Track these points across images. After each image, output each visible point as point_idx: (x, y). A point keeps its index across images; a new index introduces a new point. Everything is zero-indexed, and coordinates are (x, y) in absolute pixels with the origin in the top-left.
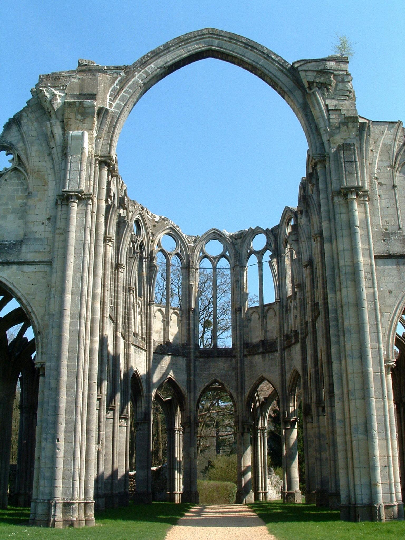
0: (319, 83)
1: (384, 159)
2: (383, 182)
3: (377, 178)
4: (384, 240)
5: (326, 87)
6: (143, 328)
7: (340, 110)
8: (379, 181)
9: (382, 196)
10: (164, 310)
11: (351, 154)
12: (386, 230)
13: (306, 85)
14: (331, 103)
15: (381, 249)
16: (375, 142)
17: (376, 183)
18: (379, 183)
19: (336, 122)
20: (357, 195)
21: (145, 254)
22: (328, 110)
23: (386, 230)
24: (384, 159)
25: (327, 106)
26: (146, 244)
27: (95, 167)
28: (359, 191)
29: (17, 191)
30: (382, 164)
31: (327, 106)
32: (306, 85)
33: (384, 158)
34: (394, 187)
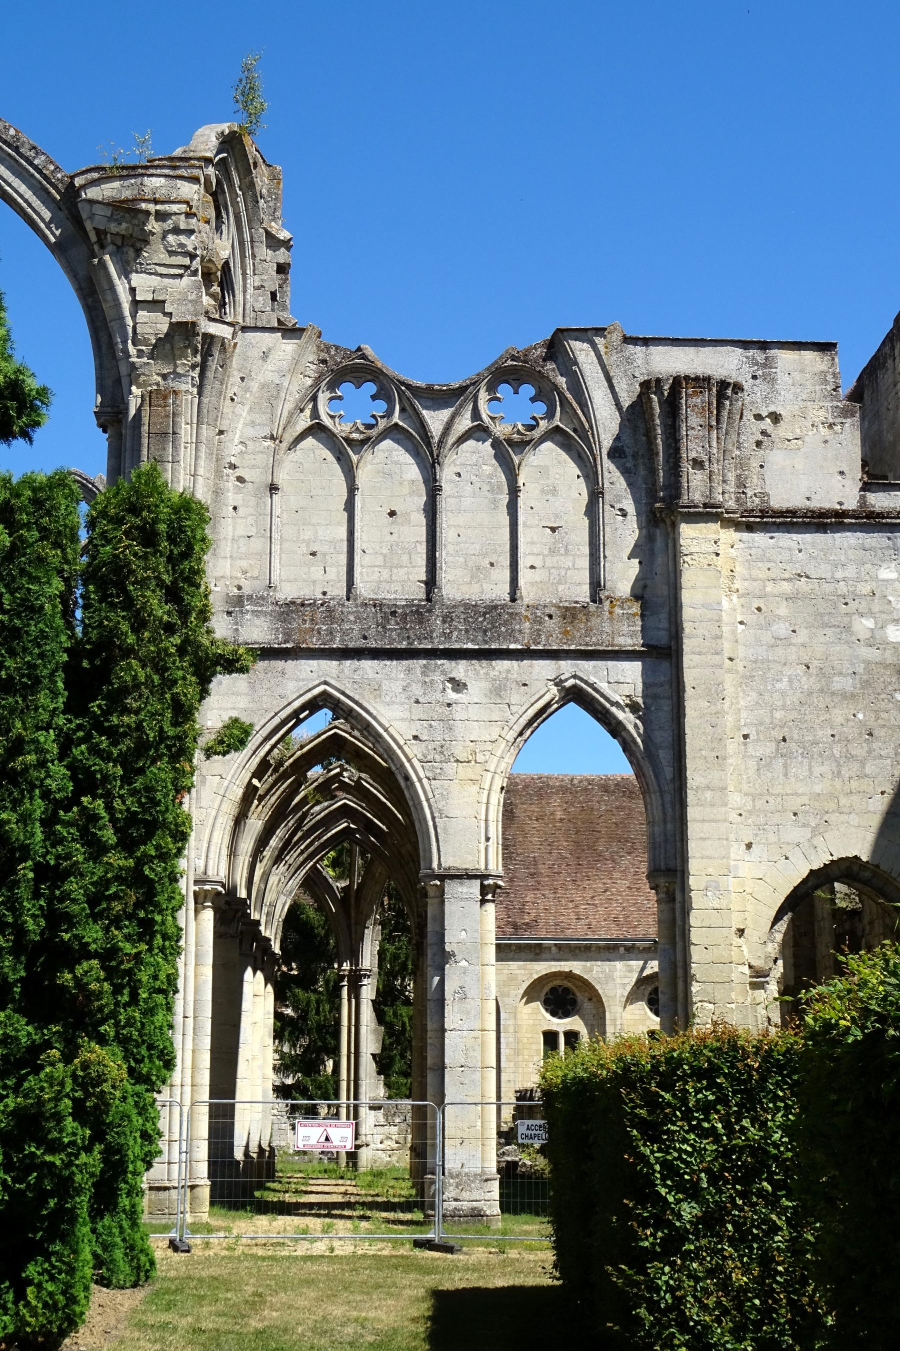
0: (117, 234)
1: (257, 421)
2: (246, 478)
3: (233, 467)
4: (229, 613)
5: (133, 246)
7: (164, 302)
8: (238, 472)
9: (241, 510)
11: (167, 416)
12: (239, 588)
13: (93, 238)
14: (145, 284)
16: (242, 379)
17: (233, 478)
18: (240, 479)
19: (151, 331)
22: (136, 305)
23: (239, 588)
24: (257, 421)
25: (133, 290)
30: (251, 432)
31: (133, 290)
32: (93, 238)
33: (259, 418)
34: (273, 488)
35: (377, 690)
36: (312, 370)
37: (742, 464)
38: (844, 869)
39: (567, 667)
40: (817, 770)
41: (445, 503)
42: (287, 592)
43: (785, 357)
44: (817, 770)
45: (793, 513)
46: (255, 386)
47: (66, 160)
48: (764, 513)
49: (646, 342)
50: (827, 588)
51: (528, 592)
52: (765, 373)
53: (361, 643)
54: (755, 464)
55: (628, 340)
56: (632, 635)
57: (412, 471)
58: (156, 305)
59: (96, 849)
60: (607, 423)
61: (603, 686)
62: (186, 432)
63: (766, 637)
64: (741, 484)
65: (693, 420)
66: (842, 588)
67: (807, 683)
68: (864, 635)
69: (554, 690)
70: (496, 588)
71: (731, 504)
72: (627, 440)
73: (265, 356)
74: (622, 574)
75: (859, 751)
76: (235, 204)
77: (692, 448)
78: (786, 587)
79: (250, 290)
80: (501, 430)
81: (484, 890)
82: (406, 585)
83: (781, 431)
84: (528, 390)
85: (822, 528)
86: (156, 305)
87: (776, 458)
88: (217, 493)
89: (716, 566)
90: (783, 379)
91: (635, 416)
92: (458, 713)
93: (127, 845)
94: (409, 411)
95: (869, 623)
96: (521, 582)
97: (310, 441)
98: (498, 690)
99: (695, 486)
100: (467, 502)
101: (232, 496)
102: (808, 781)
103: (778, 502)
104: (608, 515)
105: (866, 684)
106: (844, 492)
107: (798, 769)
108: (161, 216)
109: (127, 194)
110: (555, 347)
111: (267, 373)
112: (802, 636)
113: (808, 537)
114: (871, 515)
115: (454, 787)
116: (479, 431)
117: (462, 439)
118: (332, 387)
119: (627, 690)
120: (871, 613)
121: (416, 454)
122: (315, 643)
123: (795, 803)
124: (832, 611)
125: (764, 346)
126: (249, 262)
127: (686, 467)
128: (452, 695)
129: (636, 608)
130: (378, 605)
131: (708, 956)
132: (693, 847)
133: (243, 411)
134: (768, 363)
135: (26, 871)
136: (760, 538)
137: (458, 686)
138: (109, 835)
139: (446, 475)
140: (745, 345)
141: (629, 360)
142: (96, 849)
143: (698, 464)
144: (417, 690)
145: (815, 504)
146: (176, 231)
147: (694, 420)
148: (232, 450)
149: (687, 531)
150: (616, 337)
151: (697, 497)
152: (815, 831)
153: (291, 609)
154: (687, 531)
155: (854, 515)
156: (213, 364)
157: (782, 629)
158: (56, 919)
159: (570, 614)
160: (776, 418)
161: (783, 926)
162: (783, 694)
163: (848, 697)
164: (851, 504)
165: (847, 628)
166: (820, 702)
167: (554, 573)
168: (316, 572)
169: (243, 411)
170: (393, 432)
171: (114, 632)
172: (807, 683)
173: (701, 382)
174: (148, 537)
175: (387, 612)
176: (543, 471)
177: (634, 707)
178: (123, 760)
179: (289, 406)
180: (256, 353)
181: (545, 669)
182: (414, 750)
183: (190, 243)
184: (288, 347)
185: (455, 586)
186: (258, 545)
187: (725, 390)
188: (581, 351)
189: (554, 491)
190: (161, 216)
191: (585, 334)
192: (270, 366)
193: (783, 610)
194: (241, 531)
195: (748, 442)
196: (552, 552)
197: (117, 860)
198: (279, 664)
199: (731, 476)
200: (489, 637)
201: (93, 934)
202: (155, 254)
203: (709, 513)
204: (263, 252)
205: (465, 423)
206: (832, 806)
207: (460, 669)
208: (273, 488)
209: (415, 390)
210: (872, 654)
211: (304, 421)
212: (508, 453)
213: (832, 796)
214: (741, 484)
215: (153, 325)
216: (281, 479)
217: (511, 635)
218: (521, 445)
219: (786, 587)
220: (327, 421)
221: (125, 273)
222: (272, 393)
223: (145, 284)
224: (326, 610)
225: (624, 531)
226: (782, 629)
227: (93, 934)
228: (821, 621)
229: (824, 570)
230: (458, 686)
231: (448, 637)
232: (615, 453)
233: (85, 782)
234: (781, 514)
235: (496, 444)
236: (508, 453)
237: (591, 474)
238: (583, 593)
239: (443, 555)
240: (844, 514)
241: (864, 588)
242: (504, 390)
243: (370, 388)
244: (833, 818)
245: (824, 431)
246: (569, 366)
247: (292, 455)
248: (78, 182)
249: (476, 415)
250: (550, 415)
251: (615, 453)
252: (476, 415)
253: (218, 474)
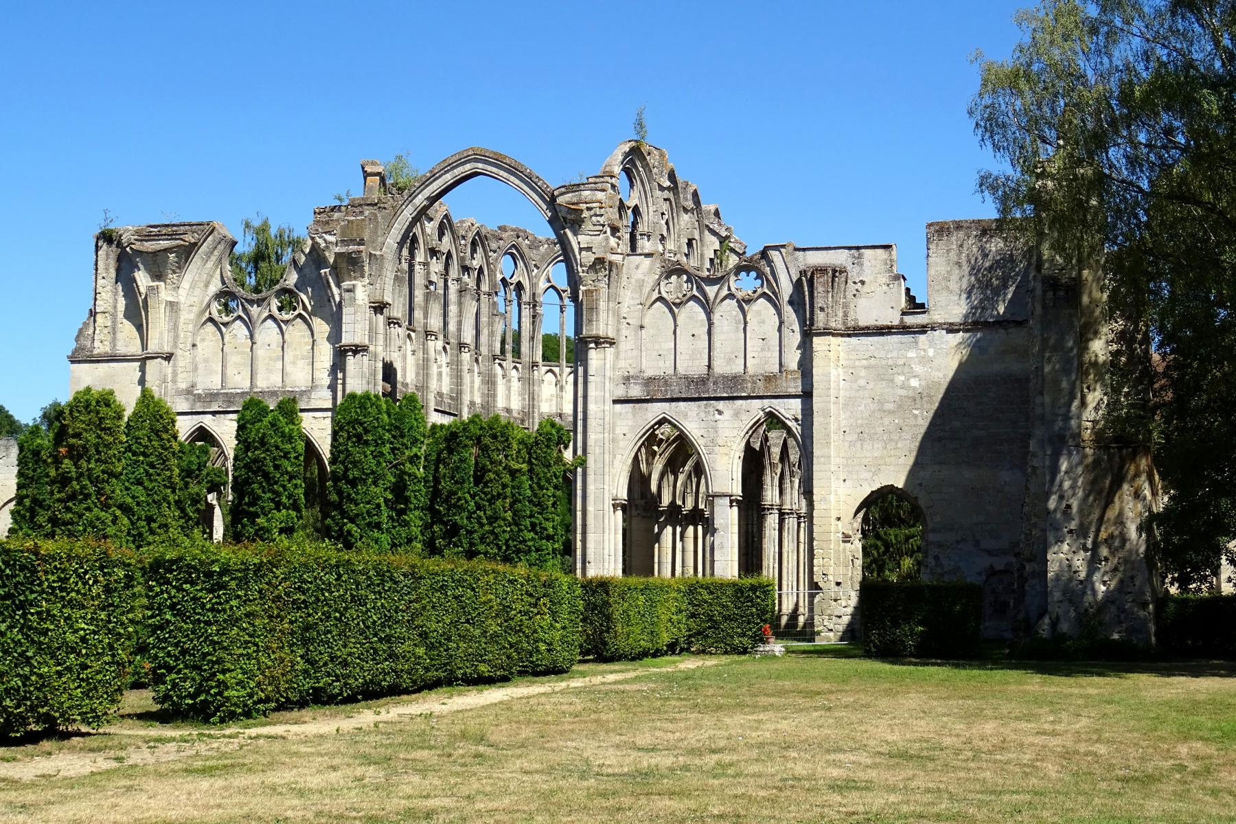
6: (524, 399)
10: (556, 370)
15: (620, 392)
20: (597, 343)
21: (526, 297)
22: (581, 249)
26: (526, 284)
27: (369, 313)
28: (598, 341)
29: (303, 336)
30: (632, 302)
34: (642, 327)
35: (686, 416)
36: (658, 271)
37: (845, 306)
38: (890, 489)
39: (766, 402)
40: (876, 446)
41: (716, 330)
42: (649, 373)
43: (867, 253)
44: (876, 446)
45: (868, 328)
46: (633, 281)
47: (553, 182)
48: (855, 329)
49: (804, 250)
50: (884, 362)
51: (751, 370)
52: (858, 261)
53: (679, 395)
54: (852, 305)
55: (796, 249)
56: (796, 387)
57: (703, 316)
58: (589, 249)
59: (482, 525)
60: (786, 289)
61: (782, 411)
62: (602, 305)
63: (855, 386)
64: (846, 315)
65: (819, 289)
66: (891, 362)
67: (873, 407)
68: (899, 384)
69: (762, 413)
70: (737, 368)
71: (839, 326)
72: (795, 297)
73: (637, 267)
74: (793, 358)
75: (895, 437)
76: (639, 175)
77: (819, 302)
78: (865, 363)
79: (651, 213)
80: (739, 295)
81: (731, 502)
82: (697, 368)
83: (866, 288)
84: (753, 274)
85: (882, 334)
86: (589, 249)
87: (862, 302)
88: (618, 331)
89: (831, 354)
90: (866, 264)
91: (798, 285)
92: (720, 424)
93: (490, 524)
94: (700, 289)
95: (902, 378)
96: (748, 364)
97: (658, 303)
98: (737, 414)
99: (820, 318)
100: (726, 328)
101: (624, 332)
102: (872, 451)
103: (862, 323)
104: (785, 331)
105: (900, 406)
106: (894, 318)
107: (867, 446)
108: (589, 209)
109: (575, 200)
110: (764, 254)
111: (638, 275)
112: (871, 386)
113: (876, 338)
114: (904, 327)
115: (718, 457)
116: (731, 296)
117: (722, 300)
118: (667, 278)
119: (793, 412)
120: (903, 373)
121: (703, 307)
122: (660, 396)
123: (866, 461)
124: (884, 373)
125: (858, 248)
126: (650, 200)
127: (817, 311)
128: (717, 416)
129: (799, 375)
130: (686, 377)
131: (821, 530)
132: (815, 482)
133: (628, 293)
134: (860, 257)
135: (463, 532)
136: (854, 340)
137: (720, 413)
138: (485, 521)
139: (716, 317)
140: (850, 248)
141: (796, 259)
142: (482, 525)
143: (822, 309)
144: (702, 415)
145: (879, 323)
146: (596, 215)
147: (820, 289)
148: (624, 311)
149: (815, 339)
150: (790, 249)
151: (821, 325)
152: (875, 474)
153: (650, 381)
154: (815, 339)
155: (897, 327)
156: (613, 274)
157: (862, 382)
158: (472, 544)
159: (769, 379)
160: (863, 282)
161: (861, 515)
162: (862, 412)
163: (890, 412)
164: (896, 322)
165: (892, 381)
166: (878, 415)
167: (762, 360)
168: (661, 364)
169: (628, 293)
170: (694, 298)
171: (484, 466)
172: (873, 407)
173: (822, 270)
174: (494, 437)
175: (689, 380)
176: (759, 313)
177: (796, 420)
178: (488, 500)
179: (648, 289)
180: (633, 266)
181: (757, 403)
182: (701, 441)
183: (601, 220)
184: (648, 261)
185: (720, 368)
186: (635, 353)
187: (836, 272)
188: (774, 255)
189: (763, 322)
190: (589, 209)
191: (776, 248)
192: (640, 271)
193: (863, 373)
194: (629, 347)
195: (849, 295)
196: (762, 350)
197: (487, 528)
198: (645, 405)
199: (840, 314)
200: (733, 389)
201: (482, 548)
202: (587, 226)
203: (827, 332)
204: (658, 193)
205: (725, 292)
206: (882, 462)
207: (721, 405)
208: (642, 327)
209: (702, 279)
210: (903, 392)
211: (655, 295)
212: (744, 303)
213: (882, 457)
214: (846, 315)
215: (588, 258)
216: (646, 322)
217: (743, 390)
218: (749, 301)
219: (865, 363)
220: (664, 295)
221: (575, 234)
222: (641, 284)
223: (584, 240)
224: (664, 381)
225: (794, 338)
226: (862, 382)
227: (482, 548)
228: (880, 377)
229: (882, 354)
230: (720, 413)
231: (715, 391)
232: (791, 302)
233: (479, 507)
234: (863, 329)
235: (738, 301)
236: (744, 303)
237: (779, 314)
238: (776, 369)
239: (715, 354)
240: (892, 327)
241: (901, 362)
242: (743, 274)
243: (685, 277)
244: (883, 467)
245: (885, 287)
246: (770, 263)
247: (651, 311)
248: (556, 193)
249: (729, 289)
250: (762, 286)
251: (791, 302)
252: (729, 289)
253: (619, 322)
